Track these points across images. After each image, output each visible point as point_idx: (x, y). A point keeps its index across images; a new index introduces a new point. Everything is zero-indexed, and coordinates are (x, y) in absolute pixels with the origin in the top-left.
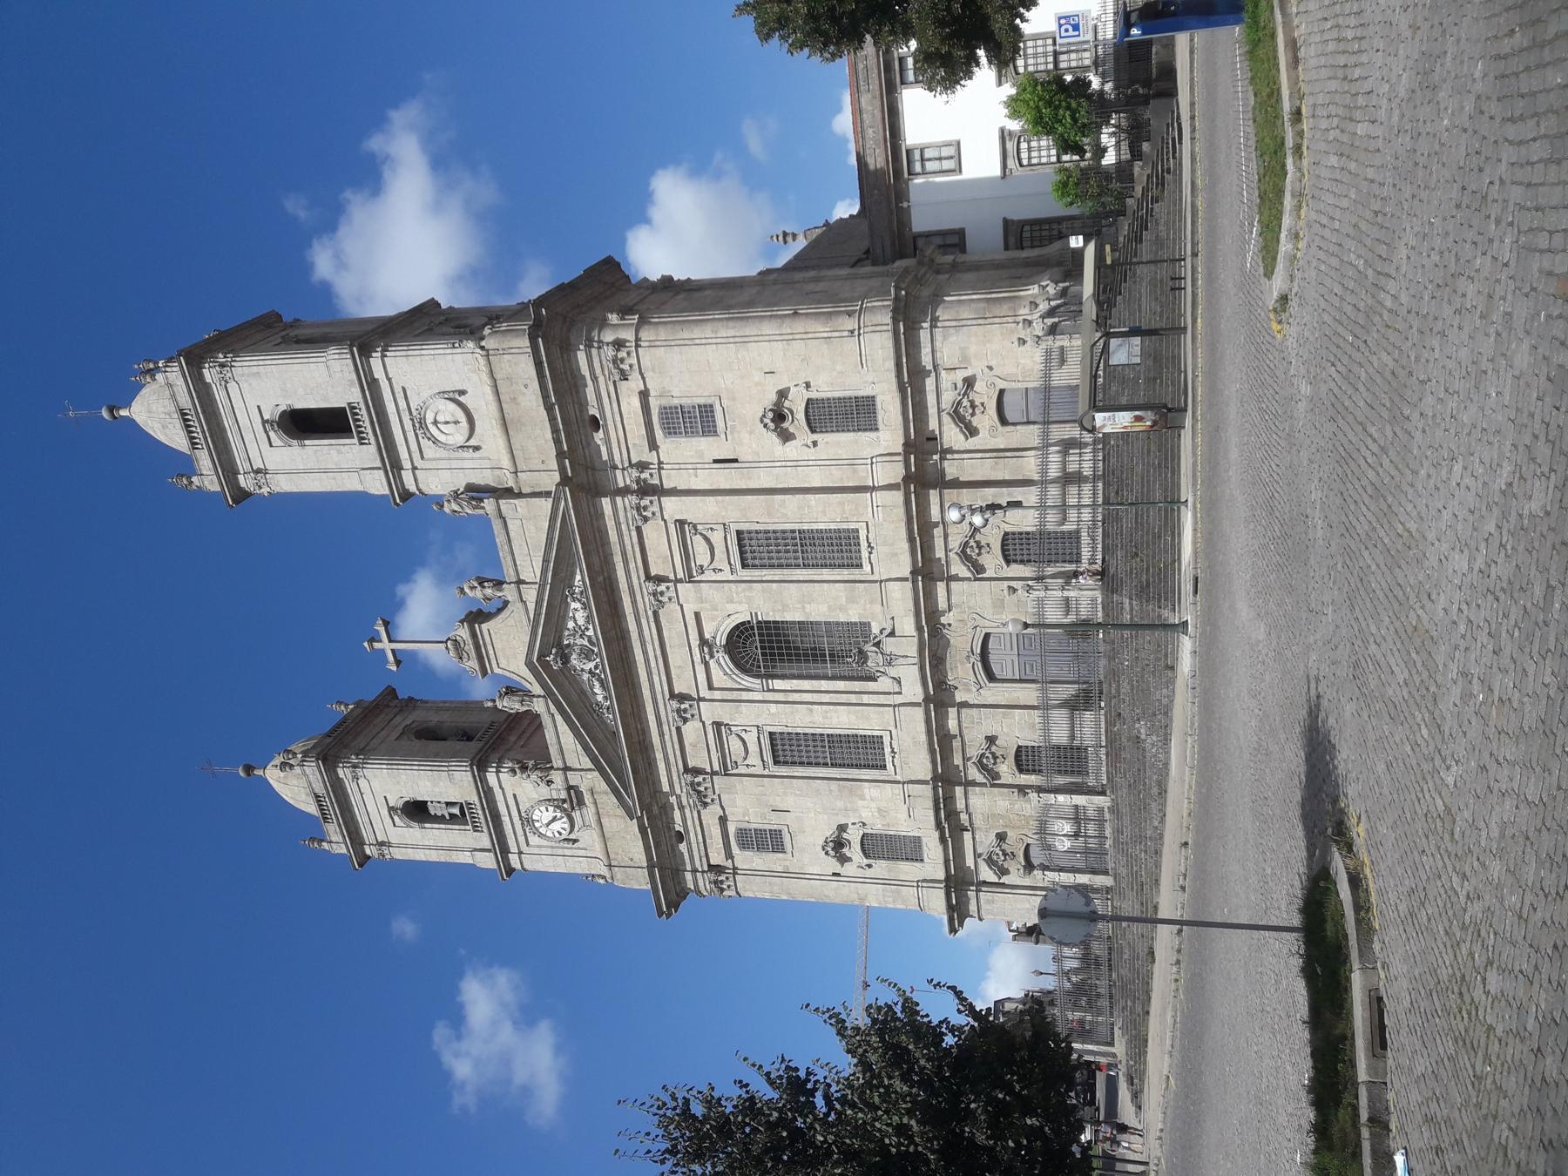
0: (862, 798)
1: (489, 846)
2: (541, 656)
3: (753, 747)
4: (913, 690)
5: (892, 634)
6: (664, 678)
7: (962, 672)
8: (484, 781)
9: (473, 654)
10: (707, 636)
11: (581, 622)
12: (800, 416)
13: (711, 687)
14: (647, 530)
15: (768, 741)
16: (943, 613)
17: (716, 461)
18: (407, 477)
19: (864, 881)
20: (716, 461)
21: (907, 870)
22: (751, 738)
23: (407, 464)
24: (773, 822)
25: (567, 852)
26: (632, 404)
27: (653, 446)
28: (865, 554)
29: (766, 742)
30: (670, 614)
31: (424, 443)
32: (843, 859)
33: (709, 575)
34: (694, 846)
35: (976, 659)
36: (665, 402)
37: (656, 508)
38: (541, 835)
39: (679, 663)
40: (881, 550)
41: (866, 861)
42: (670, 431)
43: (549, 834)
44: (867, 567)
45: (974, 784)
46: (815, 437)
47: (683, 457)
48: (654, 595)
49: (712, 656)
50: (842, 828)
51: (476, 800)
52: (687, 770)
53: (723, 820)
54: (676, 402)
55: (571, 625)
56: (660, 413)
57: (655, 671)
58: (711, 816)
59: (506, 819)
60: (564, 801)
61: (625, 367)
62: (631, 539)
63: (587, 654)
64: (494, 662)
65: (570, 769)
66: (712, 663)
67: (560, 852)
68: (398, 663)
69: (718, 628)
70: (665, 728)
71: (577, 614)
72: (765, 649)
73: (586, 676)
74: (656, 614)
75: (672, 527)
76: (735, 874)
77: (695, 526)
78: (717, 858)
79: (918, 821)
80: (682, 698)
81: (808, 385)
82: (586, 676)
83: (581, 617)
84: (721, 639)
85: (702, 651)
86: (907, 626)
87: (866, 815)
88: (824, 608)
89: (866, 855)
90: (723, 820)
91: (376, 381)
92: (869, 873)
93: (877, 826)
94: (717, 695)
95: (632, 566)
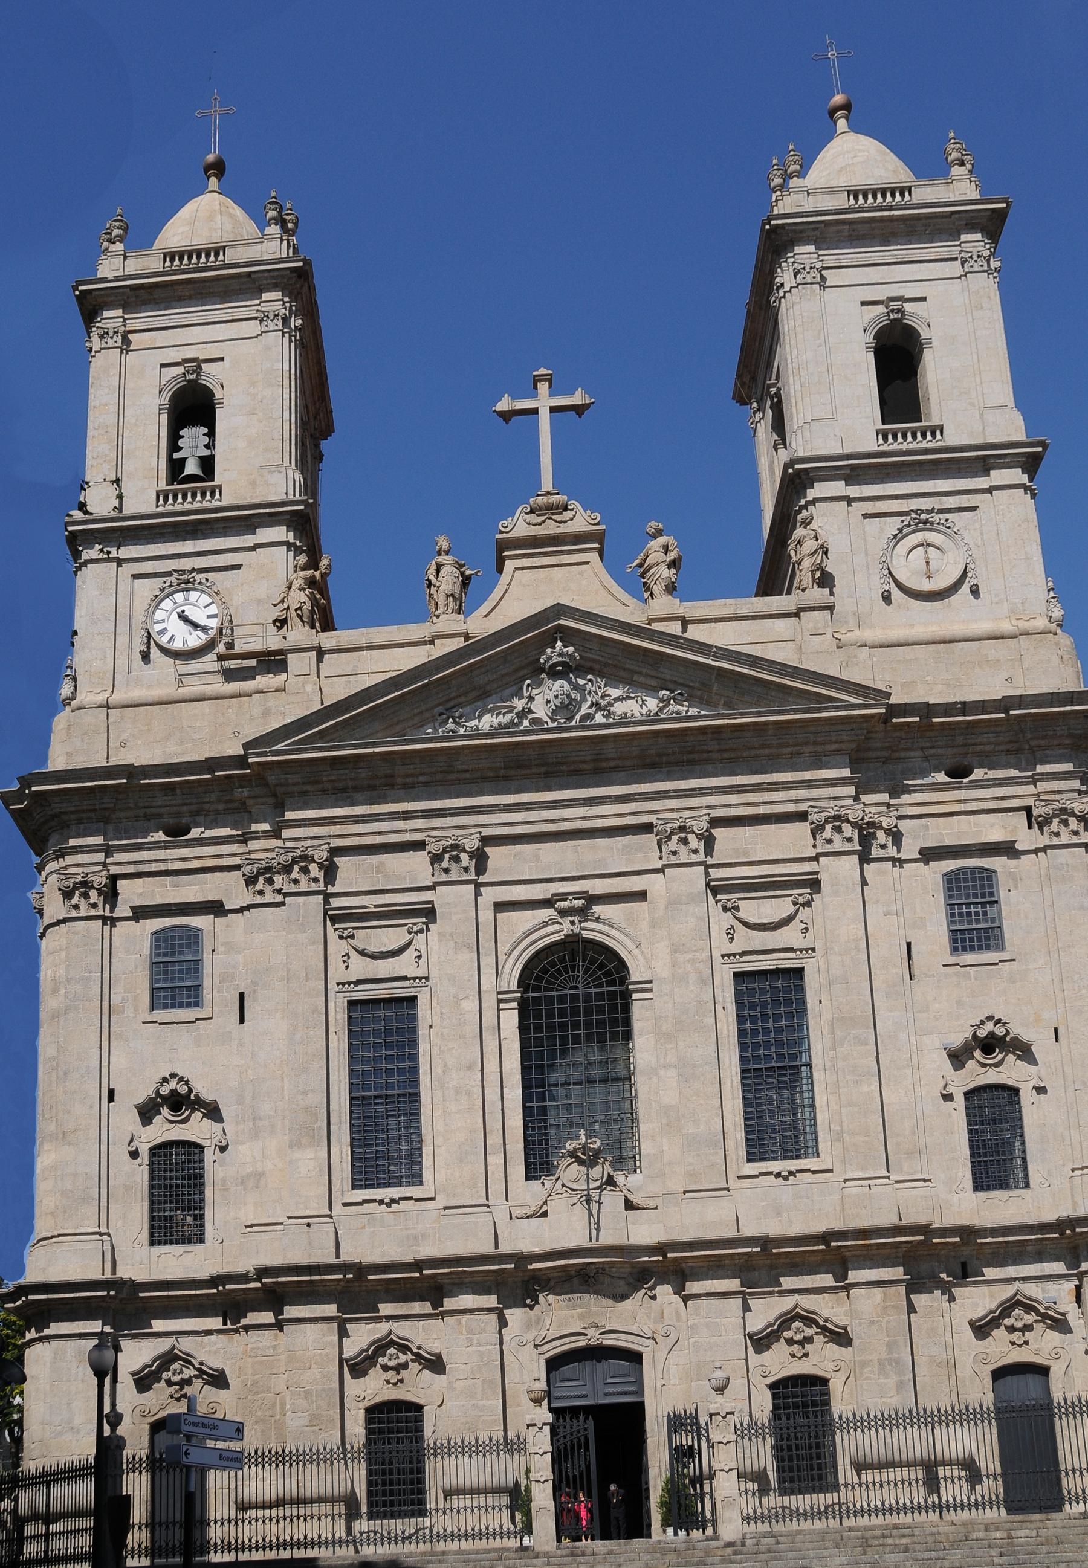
1: (128, 510)
2: (567, 635)
4: (527, 1239)
5: (629, 1206)
7: (564, 1318)
8: (272, 520)
9: (541, 531)
10: (597, 909)
11: (619, 708)
12: (992, 1077)
13: (500, 907)
14: (803, 829)
15: (397, 993)
16: (679, 1290)
17: (909, 945)
18: (837, 487)
19: (103, 1143)
20: (909, 945)
21: (132, 1217)
22: (403, 965)
23: (854, 491)
24: (217, 994)
25: (122, 640)
26: (993, 830)
27: (929, 855)
28: (775, 1166)
29: (397, 990)
30: (643, 851)
31: (892, 525)
32: (147, 1112)
33: (728, 919)
34: (161, 854)
35: (593, 1338)
36: (1001, 879)
37: (838, 845)
38: (157, 601)
40: (785, 1191)
41: (144, 1150)
42: (953, 882)
43: (159, 615)
45: (343, 1333)
46: (959, 1099)
47: (916, 900)
48: (682, 829)
49: (563, 913)
50: (213, 1112)
51: (226, 501)
52: (114, 879)
54: (1002, 894)
55: (615, 693)
56: (981, 869)
58: (230, 889)
59: (189, 546)
60: (230, 646)
61: (1055, 825)
62: (782, 801)
63: (566, 708)
64: (526, 562)
65: (320, 660)
66: (548, 913)
67: (123, 628)
68: (506, 416)
69: (613, 926)
70: (419, 823)
71: (636, 708)
73: (519, 704)
74: (648, 828)
75: (807, 867)
76: (104, 919)
77: (807, 904)
78: (131, 893)
79: (234, 1240)
80: (480, 859)
81: (1041, 1090)
82: (519, 704)
83: (631, 707)
84: (591, 931)
85: (577, 895)
86: (644, 1232)
87: (243, 1153)
88: (670, 1097)
89: (154, 1151)
90: (216, 908)
91: (986, 472)
92: (119, 1153)
93: (214, 1169)
94: (486, 915)
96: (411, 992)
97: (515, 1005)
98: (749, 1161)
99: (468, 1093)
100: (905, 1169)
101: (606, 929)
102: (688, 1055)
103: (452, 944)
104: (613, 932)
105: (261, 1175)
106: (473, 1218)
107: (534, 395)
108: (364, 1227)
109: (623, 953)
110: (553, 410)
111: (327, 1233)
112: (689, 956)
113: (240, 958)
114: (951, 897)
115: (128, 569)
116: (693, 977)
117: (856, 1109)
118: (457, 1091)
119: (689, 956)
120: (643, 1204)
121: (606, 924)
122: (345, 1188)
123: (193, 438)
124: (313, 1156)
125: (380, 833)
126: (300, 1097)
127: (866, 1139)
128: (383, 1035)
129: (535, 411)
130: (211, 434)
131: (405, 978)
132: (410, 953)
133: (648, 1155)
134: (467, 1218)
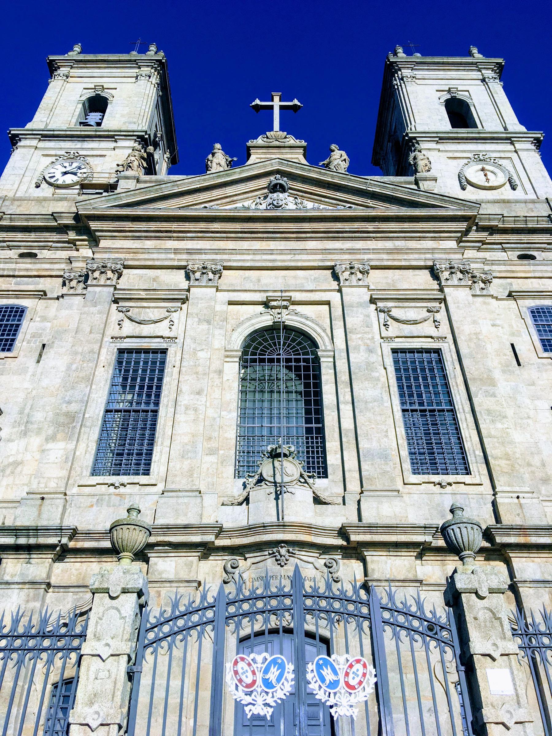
0: (52, 438)
3: (146, 330)
17: (512, 345)
20: (512, 345)
22: (162, 329)
28: (436, 478)
29: (155, 344)
34: (13, 266)
39: (264, 281)
53: (43, 295)
57: (258, 257)
58: (53, 286)
69: (307, 318)
70: (185, 257)
72: (283, 359)
90: (43, 295)
95: (385, 256)
96: (164, 346)
97: (237, 360)
98: (414, 473)
99: (196, 410)
100: (543, 492)
101: (303, 320)
102: (361, 394)
103: (197, 320)
104: (308, 322)
105: (21, 463)
106: (186, 500)
108: (92, 506)
109: (314, 335)
110: (281, 107)
111: (57, 507)
112: (359, 336)
113: (49, 325)
114: (535, 321)
115: (39, 153)
116: (362, 348)
117: (495, 440)
118: (187, 409)
119: (359, 336)
121: (303, 318)
122: (84, 474)
123: (94, 117)
124: (64, 447)
126: (65, 405)
127: (508, 462)
128: (141, 374)
129: (272, 107)
130: (103, 116)
131: (162, 337)
132: (166, 323)
133: (333, 465)
134: (181, 500)
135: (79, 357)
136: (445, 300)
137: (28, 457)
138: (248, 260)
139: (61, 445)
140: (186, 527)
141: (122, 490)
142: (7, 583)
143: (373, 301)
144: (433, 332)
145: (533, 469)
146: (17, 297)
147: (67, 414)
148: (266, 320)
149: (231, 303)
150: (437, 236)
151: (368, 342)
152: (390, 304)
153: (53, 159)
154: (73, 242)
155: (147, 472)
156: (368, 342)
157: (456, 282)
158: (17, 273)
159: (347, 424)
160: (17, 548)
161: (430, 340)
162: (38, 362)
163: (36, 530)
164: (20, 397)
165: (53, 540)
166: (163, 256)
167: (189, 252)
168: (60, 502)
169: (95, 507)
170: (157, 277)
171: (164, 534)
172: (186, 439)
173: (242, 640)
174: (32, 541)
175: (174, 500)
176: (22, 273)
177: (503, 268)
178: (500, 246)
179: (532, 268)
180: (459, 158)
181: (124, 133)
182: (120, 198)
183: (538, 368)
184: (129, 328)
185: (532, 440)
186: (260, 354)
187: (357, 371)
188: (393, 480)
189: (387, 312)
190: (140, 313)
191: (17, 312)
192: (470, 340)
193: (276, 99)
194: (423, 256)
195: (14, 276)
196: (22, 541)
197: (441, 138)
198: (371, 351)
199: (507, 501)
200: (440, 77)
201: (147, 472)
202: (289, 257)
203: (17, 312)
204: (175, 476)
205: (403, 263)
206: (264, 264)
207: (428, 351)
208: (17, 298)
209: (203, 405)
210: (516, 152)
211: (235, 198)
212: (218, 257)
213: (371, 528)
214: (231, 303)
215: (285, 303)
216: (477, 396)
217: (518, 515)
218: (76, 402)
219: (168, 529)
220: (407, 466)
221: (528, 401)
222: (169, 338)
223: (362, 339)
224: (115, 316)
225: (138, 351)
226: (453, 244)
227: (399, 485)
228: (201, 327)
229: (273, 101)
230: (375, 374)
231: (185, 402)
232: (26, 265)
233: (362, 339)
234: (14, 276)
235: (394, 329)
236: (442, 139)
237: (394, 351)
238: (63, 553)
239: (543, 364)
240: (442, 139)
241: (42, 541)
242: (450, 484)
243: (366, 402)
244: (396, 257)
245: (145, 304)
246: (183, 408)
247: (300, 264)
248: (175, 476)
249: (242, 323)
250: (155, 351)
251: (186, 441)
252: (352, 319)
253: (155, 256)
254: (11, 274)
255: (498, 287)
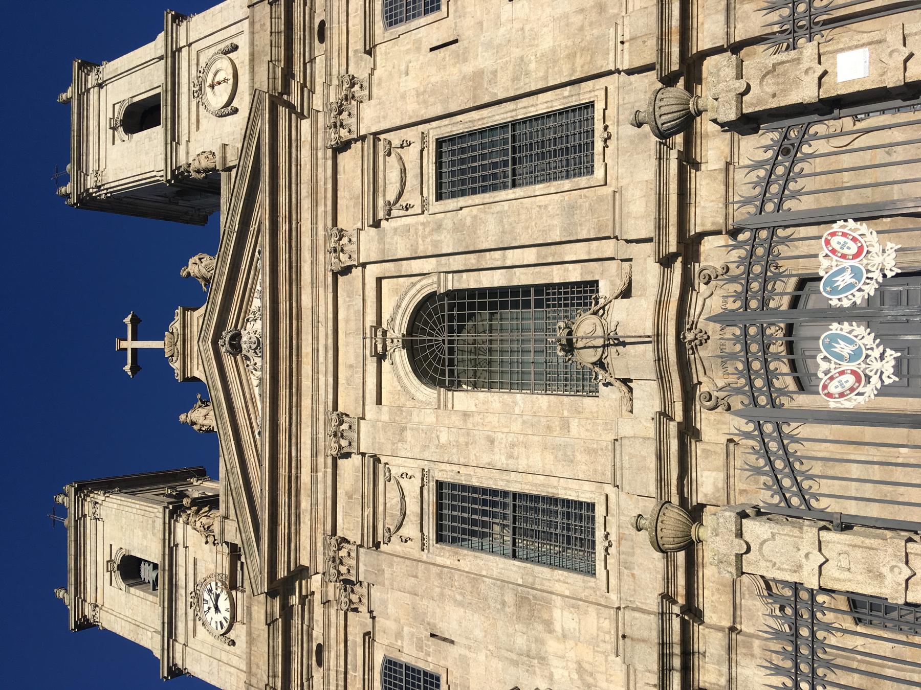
0: (548, 625)
3: (413, 507)
6: (331, 380)
15: (433, 498)
17: (432, 50)
20: (432, 50)
22: (412, 487)
28: (598, 145)
29: (431, 496)
34: (333, 674)
39: (352, 361)
44: (599, 172)
57: (322, 368)
58: (358, 624)
68: (134, 368)
70: (321, 459)
90: (369, 637)
95: (321, 209)
96: (433, 485)
97: (450, 393)
98: (593, 172)
99: (513, 445)
100: (616, 11)
101: (401, 311)
102: (494, 238)
103: (400, 444)
104: (403, 305)
105: (579, 663)
106: (626, 458)
107: (126, 349)
108: (633, 575)
109: (419, 297)
110: (134, 338)
111: (634, 618)
112: (420, 241)
113: (406, 629)
114: (401, 21)
117: (550, 71)
118: (511, 456)
119: (420, 241)
120: (625, 280)
121: (397, 311)
122: (592, 584)
123: (146, 573)
124: (559, 611)
125: (325, 493)
126: (507, 609)
127: (578, 55)
128: (466, 514)
130: (146, 561)
131: (422, 488)
132: (404, 483)
133: (581, 274)
135: (447, 592)
136: (376, 135)
137: (571, 655)
138: (324, 380)
139: (557, 613)
140: (659, 457)
141: (613, 538)
142: (730, 681)
143: (376, 224)
144: (414, 150)
145: (586, 24)
146: (371, 669)
147: (518, 606)
148: (401, 357)
149: (379, 402)
150: (294, 143)
151: (427, 230)
152: (381, 203)
153: (199, 623)
154: (303, 599)
155: (591, 506)
156: (427, 230)
157: (353, 120)
158: (342, 669)
159: (530, 256)
160: (687, 670)
161: (425, 153)
162: (452, 642)
163: (664, 645)
164: (497, 664)
165: (676, 624)
166: (320, 486)
167: (315, 454)
168: (629, 615)
169: (635, 572)
170: (347, 493)
171: (669, 485)
172: (550, 458)
173: (801, 387)
174: (677, 650)
175: (626, 473)
176: (342, 663)
177: (335, 62)
178: (308, 66)
179: (335, 25)
180: (198, 116)
181: (167, 534)
182: (249, 539)
183: (460, 17)
184: (410, 529)
185: (551, 25)
186: (443, 365)
187: (464, 244)
188: (601, 199)
189: (390, 207)
190: (392, 515)
191: (390, 669)
192: (425, 102)
193: (124, 344)
194: (321, 162)
195: (346, 673)
196: (677, 662)
197: (173, 139)
198: (439, 227)
199: (626, 57)
200: (96, 140)
201: (591, 506)
202: (322, 329)
203: (390, 669)
204: (595, 471)
205: (330, 186)
206: (331, 360)
207: (439, 155)
208: (373, 668)
209: (506, 435)
210: (190, 45)
211: (248, 396)
212: (322, 417)
213: (661, 225)
214: (379, 402)
215: (379, 334)
216: (496, 94)
217: (644, 42)
218: (503, 595)
219: (661, 481)
220: (583, 181)
221: (502, 30)
222: (423, 479)
223: (424, 238)
224: (395, 546)
225: (439, 517)
226: (305, 124)
227: (607, 190)
228: (409, 440)
229: (126, 349)
230: (468, 221)
231: (503, 458)
232: (332, 657)
233: (424, 238)
234: (346, 673)
235: (412, 198)
236: (173, 138)
237: (439, 197)
238: (693, 612)
239: (456, 11)
240: (173, 138)
241: (676, 637)
242: (606, 128)
243: (503, 232)
244: (321, 195)
245: (381, 508)
246: (511, 461)
247: (330, 316)
248: (595, 471)
249: (404, 387)
250: (440, 496)
251: (552, 458)
252: (399, 250)
253: (320, 496)
254: (342, 676)
255: (360, 70)
